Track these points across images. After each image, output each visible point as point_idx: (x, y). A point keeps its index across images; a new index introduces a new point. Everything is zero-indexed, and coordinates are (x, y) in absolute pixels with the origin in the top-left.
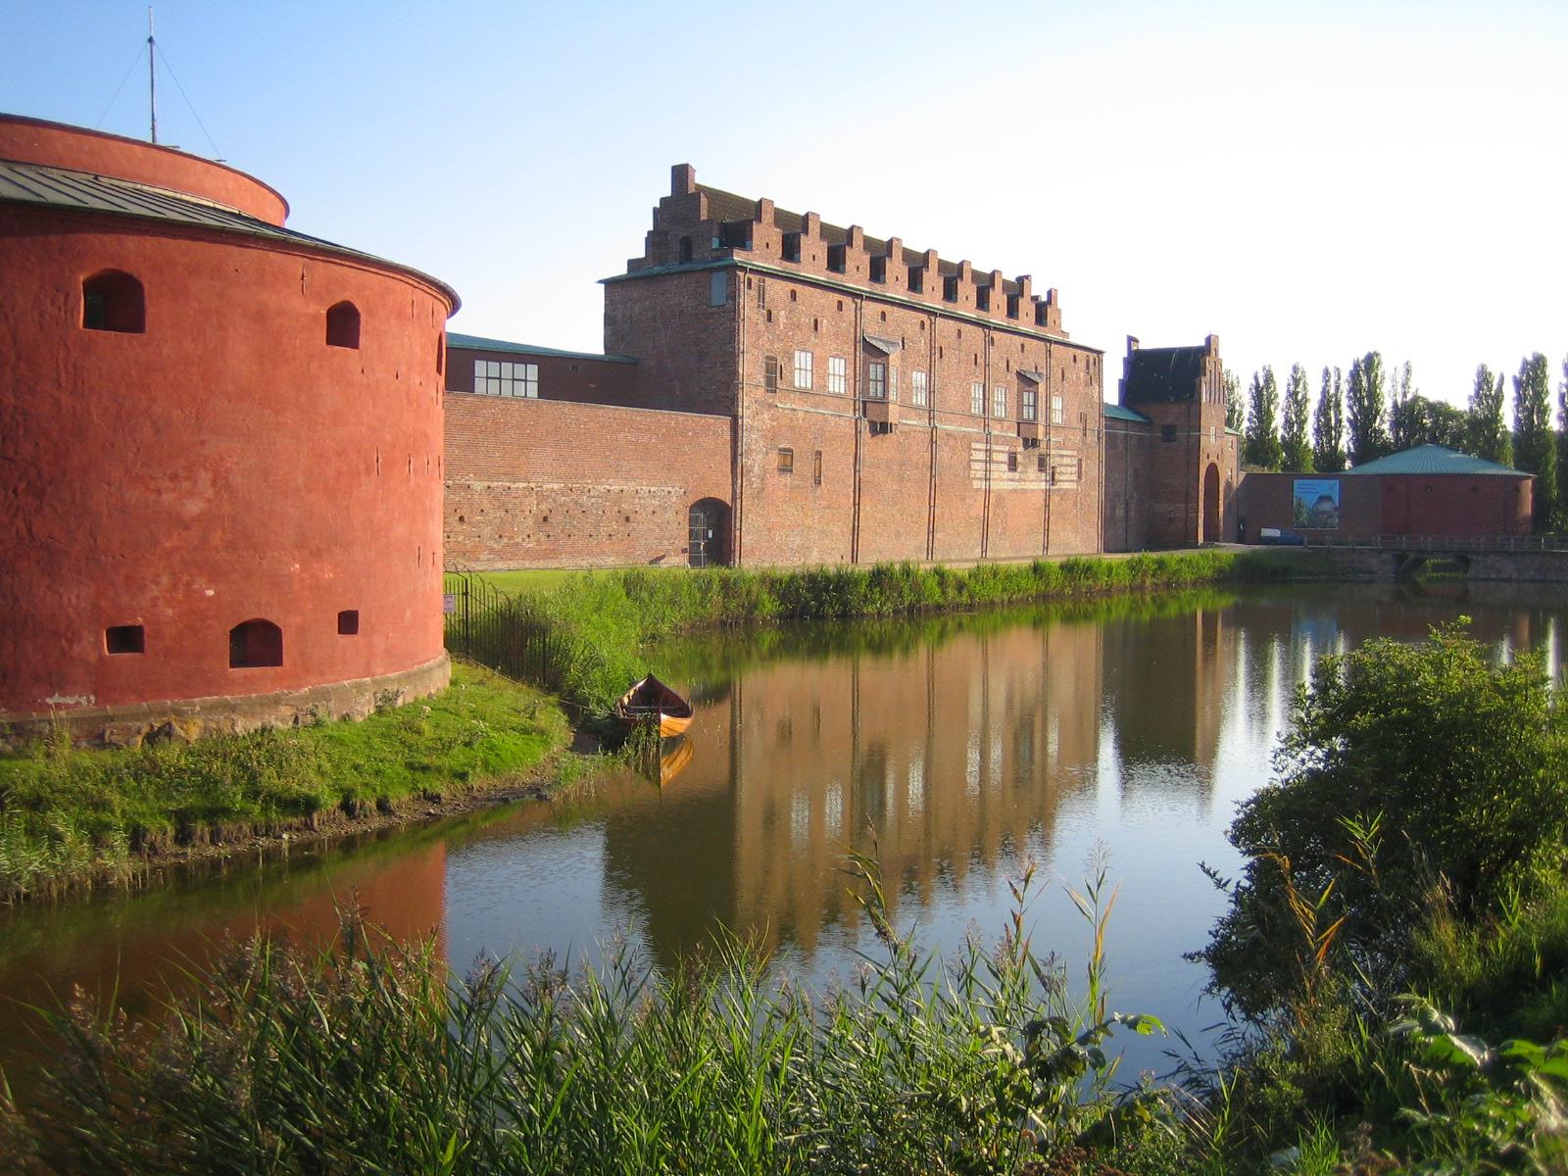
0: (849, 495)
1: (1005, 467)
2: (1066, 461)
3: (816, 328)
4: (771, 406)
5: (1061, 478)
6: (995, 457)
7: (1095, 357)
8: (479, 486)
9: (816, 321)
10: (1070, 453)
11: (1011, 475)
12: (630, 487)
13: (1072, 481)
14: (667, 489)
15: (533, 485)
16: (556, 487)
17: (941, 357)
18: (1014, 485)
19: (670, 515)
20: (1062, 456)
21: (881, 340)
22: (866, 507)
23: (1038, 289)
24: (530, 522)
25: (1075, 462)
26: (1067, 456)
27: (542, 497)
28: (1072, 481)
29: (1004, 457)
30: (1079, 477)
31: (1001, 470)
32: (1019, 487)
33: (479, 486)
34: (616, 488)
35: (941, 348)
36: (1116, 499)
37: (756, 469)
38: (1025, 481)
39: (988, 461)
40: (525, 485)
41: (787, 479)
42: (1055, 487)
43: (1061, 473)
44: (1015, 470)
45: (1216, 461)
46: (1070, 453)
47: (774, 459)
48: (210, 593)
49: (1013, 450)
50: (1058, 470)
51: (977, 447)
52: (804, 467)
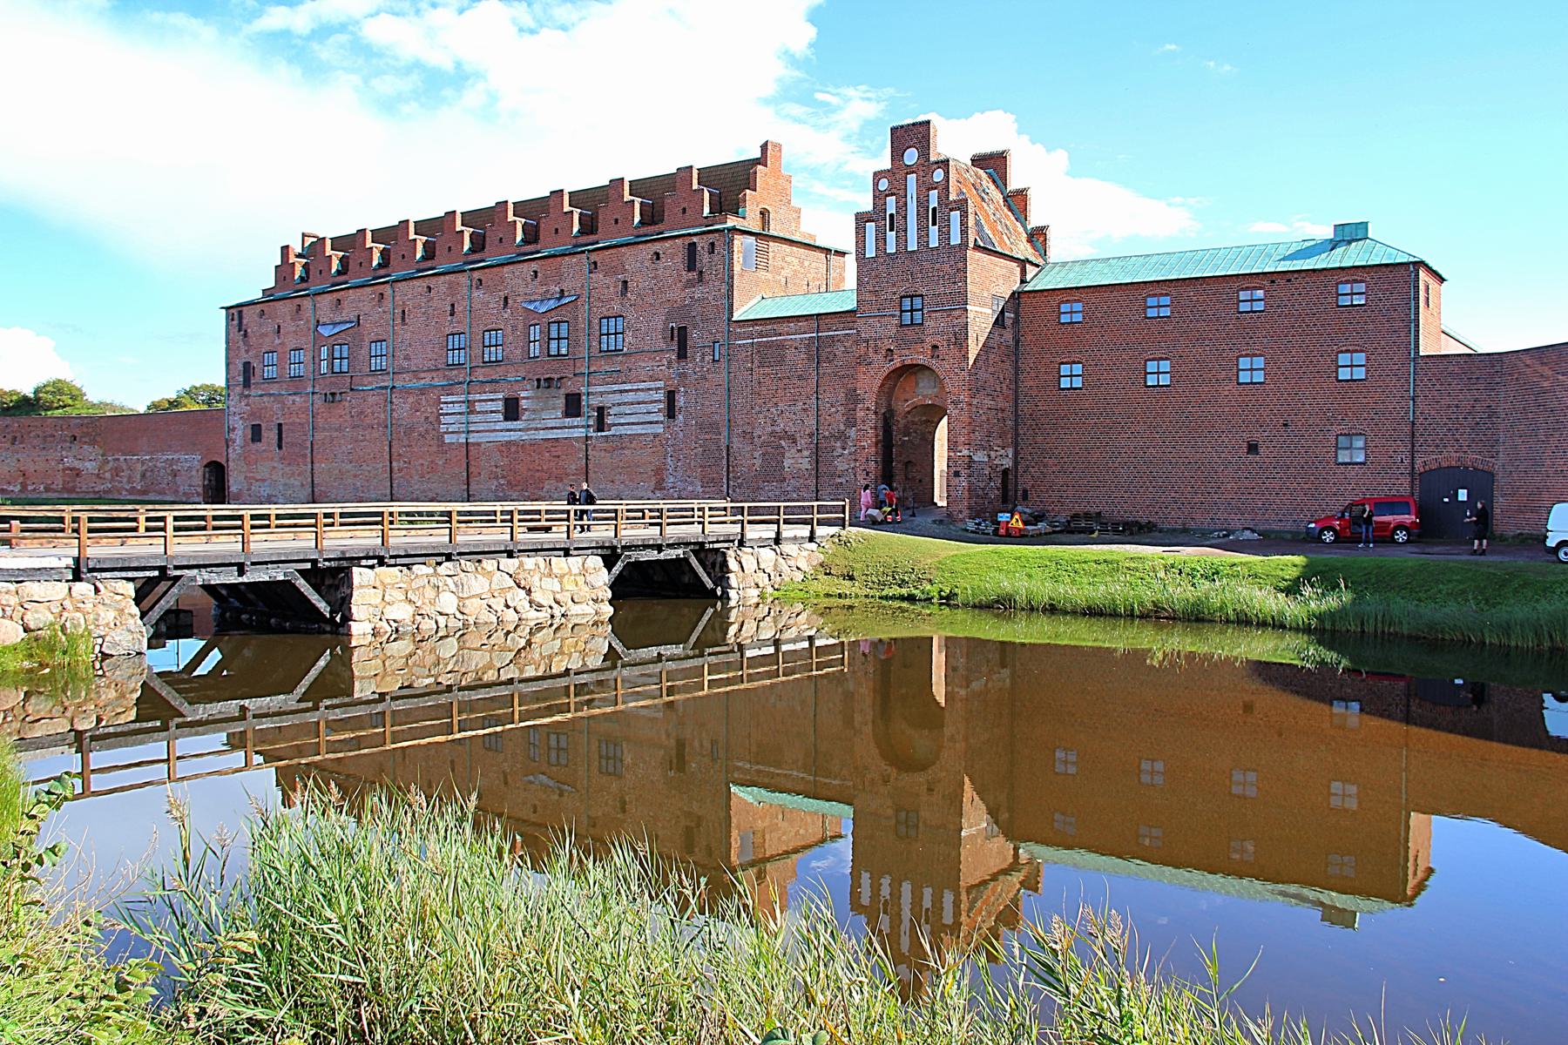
0: (306, 455)
1: (501, 417)
2: (630, 397)
3: (279, 332)
4: (247, 396)
5: (622, 421)
8: (122, 458)
9: (279, 327)
10: (642, 386)
11: (510, 425)
12: (176, 457)
13: (657, 422)
17: (403, 319)
18: (514, 436)
19: (194, 473)
20: (621, 392)
24: (138, 477)
25: (661, 396)
26: (642, 390)
27: (143, 463)
28: (657, 422)
29: (500, 406)
30: (671, 413)
32: (526, 437)
33: (122, 458)
34: (170, 457)
35: (404, 311)
36: (783, 442)
38: (536, 429)
42: (603, 434)
44: (516, 419)
45: (921, 359)
46: (642, 386)
47: (249, 432)
49: (513, 394)
52: (270, 436)
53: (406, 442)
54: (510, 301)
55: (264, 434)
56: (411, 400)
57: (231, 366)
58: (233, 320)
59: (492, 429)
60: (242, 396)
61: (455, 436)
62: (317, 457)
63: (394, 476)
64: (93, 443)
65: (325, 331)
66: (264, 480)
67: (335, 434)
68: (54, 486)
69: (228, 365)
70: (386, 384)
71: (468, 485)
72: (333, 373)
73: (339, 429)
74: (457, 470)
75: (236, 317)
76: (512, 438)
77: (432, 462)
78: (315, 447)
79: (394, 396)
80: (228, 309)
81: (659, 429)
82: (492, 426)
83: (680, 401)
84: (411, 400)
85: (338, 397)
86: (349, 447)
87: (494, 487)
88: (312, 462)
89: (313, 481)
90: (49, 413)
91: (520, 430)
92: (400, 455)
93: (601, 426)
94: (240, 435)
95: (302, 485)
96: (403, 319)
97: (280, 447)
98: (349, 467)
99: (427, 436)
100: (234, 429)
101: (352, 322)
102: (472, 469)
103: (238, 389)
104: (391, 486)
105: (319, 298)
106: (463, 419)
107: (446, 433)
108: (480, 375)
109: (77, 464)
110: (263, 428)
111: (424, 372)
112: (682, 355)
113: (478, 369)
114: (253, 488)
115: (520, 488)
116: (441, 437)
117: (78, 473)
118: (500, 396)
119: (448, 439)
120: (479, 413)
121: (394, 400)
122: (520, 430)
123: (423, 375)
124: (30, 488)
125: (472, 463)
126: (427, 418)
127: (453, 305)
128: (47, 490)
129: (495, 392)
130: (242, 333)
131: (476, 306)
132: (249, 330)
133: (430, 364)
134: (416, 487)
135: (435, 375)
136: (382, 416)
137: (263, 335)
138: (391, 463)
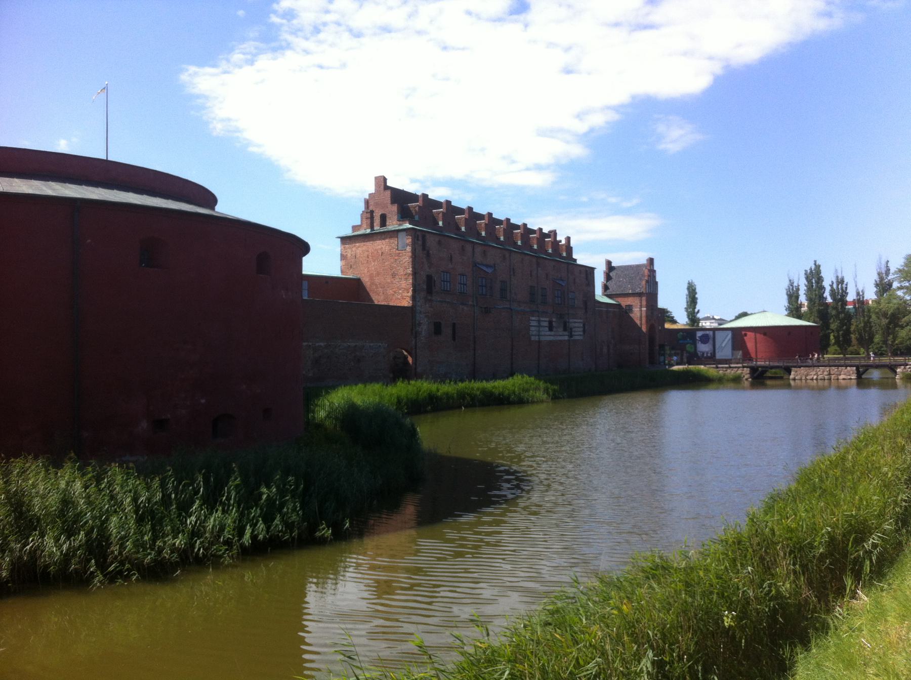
1: (547, 329)
2: (577, 325)
3: (451, 260)
5: (575, 334)
7: (589, 272)
10: (579, 321)
14: (379, 344)
15: (311, 344)
16: (322, 344)
17: (514, 273)
18: (551, 338)
20: (575, 322)
21: (484, 265)
23: (561, 238)
29: (546, 324)
30: (584, 331)
31: (545, 331)
34: (353, 344)
37: (423, 333)
43: (575, 331)
48: (203, 401)
50: (574, 330)
58: (418, 240)
59: (547, 336)
69: (415, 273)
70: (506, 306)
75: (420, 238)
81: (581, 338)
83: (586, 328)
93: (571, 336)
94: (425, 328)
96: (514, 273)
97: (454, 339)
100: (420, 324)
106: (537, 329)
112: (586, 312)
119: (533, 338)
127: (531, 272)
130: (425, 252)
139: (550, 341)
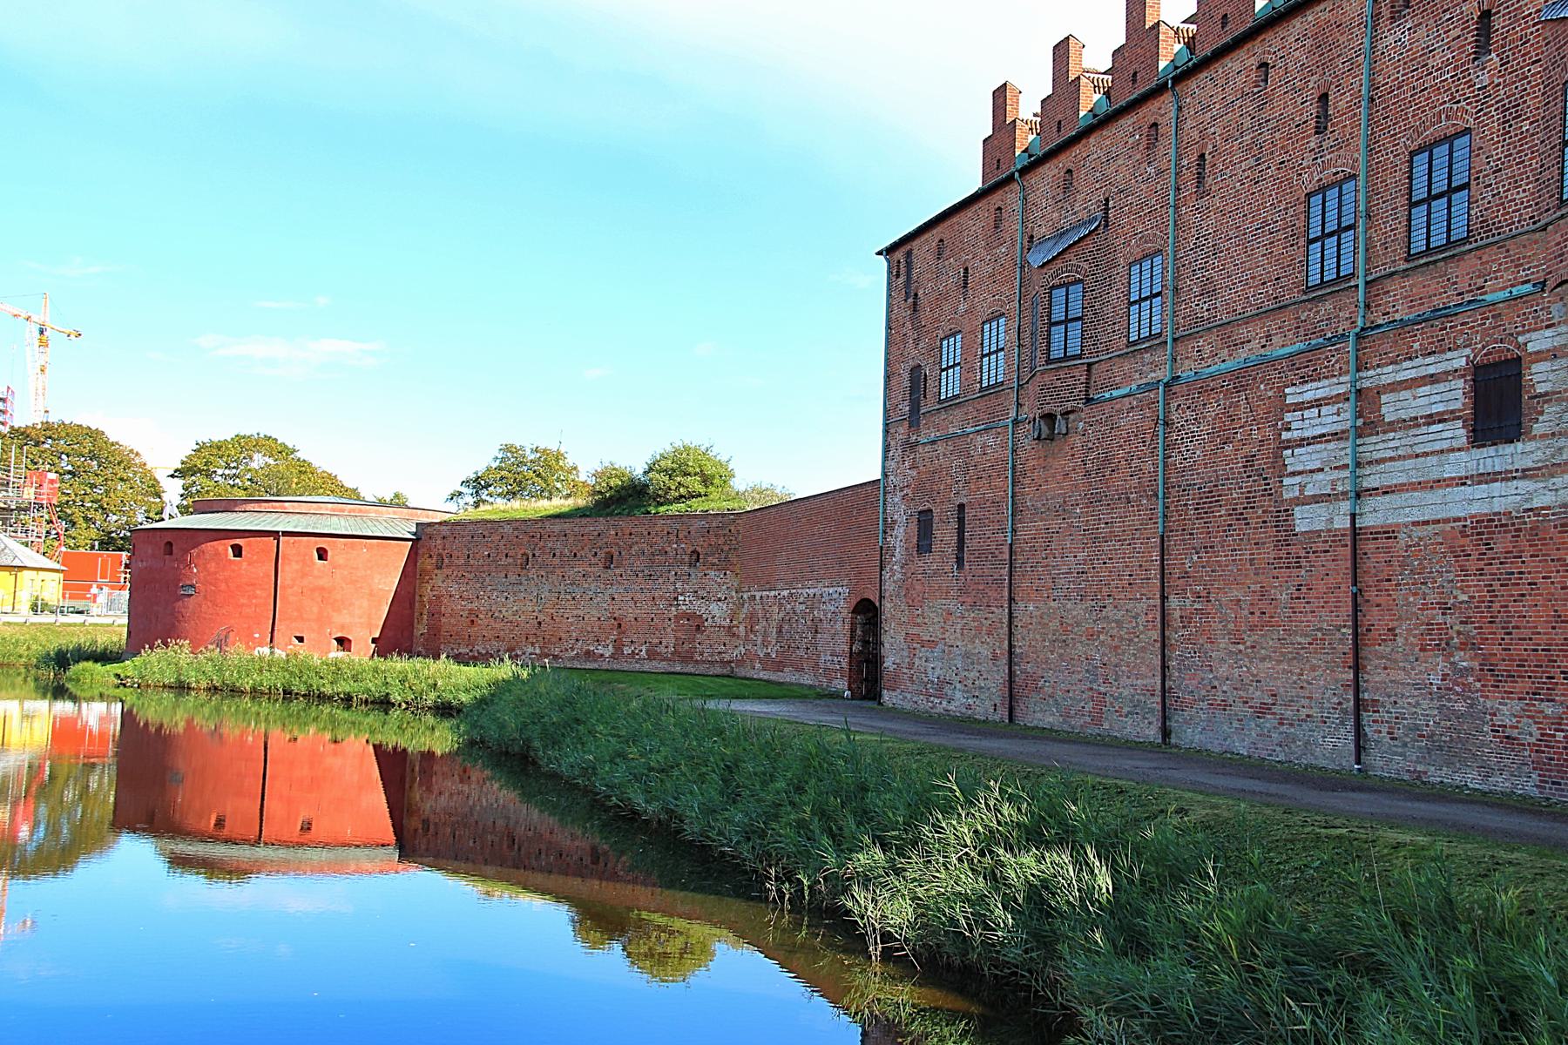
6: (1391, 408)
8: (758, 595)
9: (966, 269)
17: (1200, 178)
18: (1502, 498)
19: (839, 626)
22: (1027, 609)
29: (1456, 395)
32: (1546, 499)
33: (758, 595)
34: (811, 591)
35: (1202, 156)
39: (1368, 422)
40: (773, 593)
41: (929, 558)
51: (1309, 396)
52: (945, 534)
53: (1199, 539)
54: (1498, 23)
55: (937, 534)
56: (1212, 411)
57: (893, 382)
60: (911, 446)
61: (1321, 510)
62: (1023, 584)
63: (1174, 637)
64: (724, 566)
65: (1036, 259)
66: (932, 643)
67: (1055, 524)
68: (662, 649)
70: (1159, 374)
71: (1357, 668)
72: (1049, 361)
73: (1063, 510)
74: (1326, 620)
76: (1498, 506)
77: (1263, 593)
78: (1020, 559)
79: (1174, 405)
80: (889, 251)
82: (1432, 468)
84: (1212, 411)
85: (1060, 426)
86: (1081, 556)
87: (1436, 680)
88: (1011, 599)
89: (1011, 646)
90: (662, 509)
91: (1525, 474)
92: (1185, 575)
94: (901, 537)
95: (995, 658)
96: (1200, 178)
97: (960, 561)
98: (1078, 610)
99: (1248, 514)
100: (894, 522)
101: (1091, 222)
102: (1372, 616)
103: (902, 430)
104: (1164, 667)
105: (1033, 179)
107: (1302, 501)
108: (1398, 303)
109: (699, 607)
110: (936, 520)
111: (1248, 321)
113: (1393, 286)
114: (917, 662)
115: (1523, 685)
116: (1283, 517)
117: (697, 624)
118: (1458, 360)
119: (1306, 520)
120: (1392, 427)
121: (1174, 416)
122: (1525, 474)
123: (1243, 332)
124: (627, 651)
125: (1371, 594)
126: (1250, 459)
128: (652, 655)
129: (1437, 349)
131: (1390, 74)
132: (920, 292)
133: (1261, 297)
134: (1223, 670)
135: (1272, 325)
136: (1149, 467)
137: (943, 297)
138: (1164, 598)
139: (1484, 527)
